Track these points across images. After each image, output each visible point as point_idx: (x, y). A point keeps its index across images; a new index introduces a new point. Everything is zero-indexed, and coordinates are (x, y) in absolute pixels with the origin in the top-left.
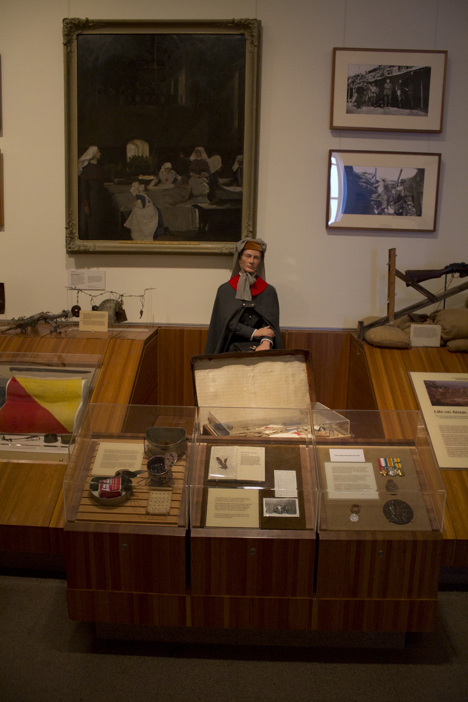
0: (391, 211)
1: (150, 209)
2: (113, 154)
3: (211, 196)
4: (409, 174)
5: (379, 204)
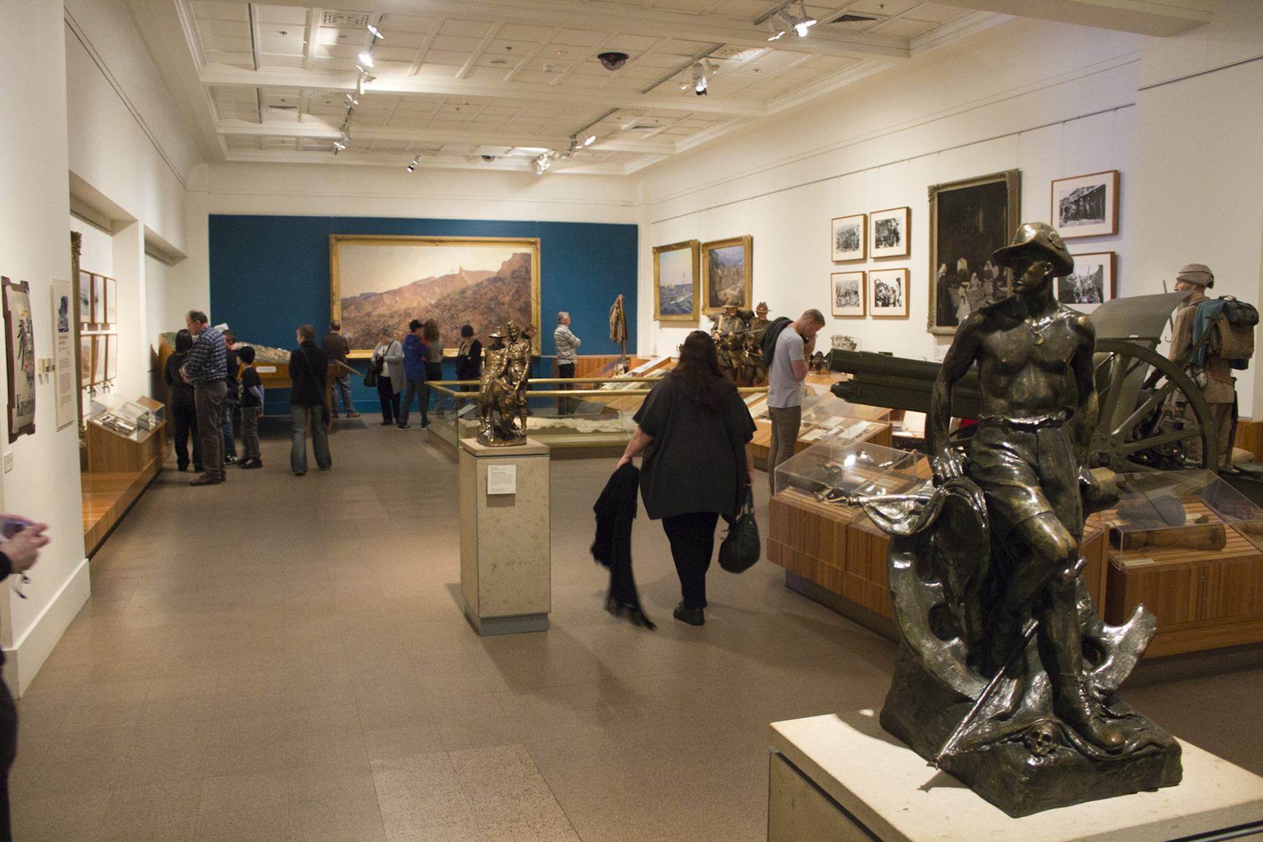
0: (1085, 300)
1: (967, 305)
2: (952, 268)
3: (994, 295)
4: (1094, 270)
5: (1078, 295)
